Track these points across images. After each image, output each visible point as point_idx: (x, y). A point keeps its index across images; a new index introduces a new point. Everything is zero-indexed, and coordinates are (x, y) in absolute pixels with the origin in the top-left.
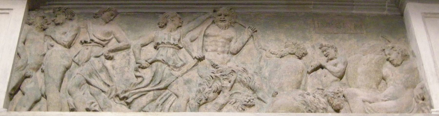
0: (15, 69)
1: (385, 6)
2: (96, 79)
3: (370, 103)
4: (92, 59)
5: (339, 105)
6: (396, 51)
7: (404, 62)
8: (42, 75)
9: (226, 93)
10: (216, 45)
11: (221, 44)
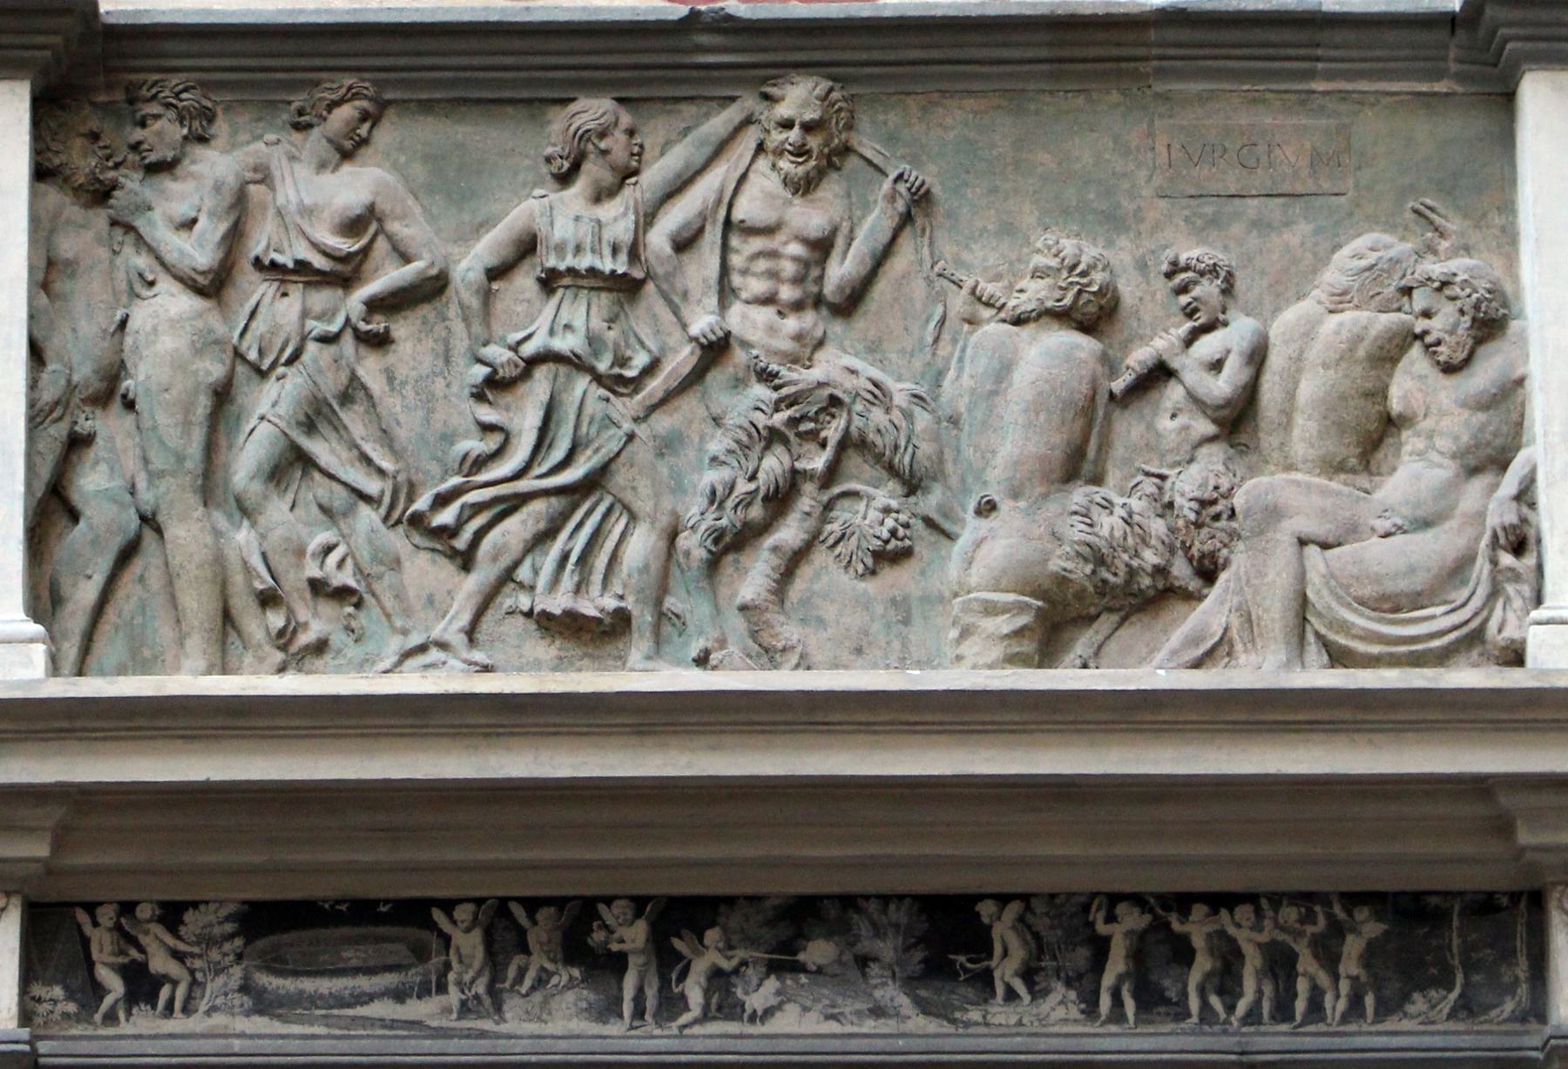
0: (36, 418)
1: (1445, 59)
2: (333, 436)
3: (1325, 546)
4: (312, 348)
5: (1212, 555)
6: (1453, 299)
7: (1482, 350)
8: (130, 419)
9: (808, 500)
10: (773, 275)
11: (789, 268)
